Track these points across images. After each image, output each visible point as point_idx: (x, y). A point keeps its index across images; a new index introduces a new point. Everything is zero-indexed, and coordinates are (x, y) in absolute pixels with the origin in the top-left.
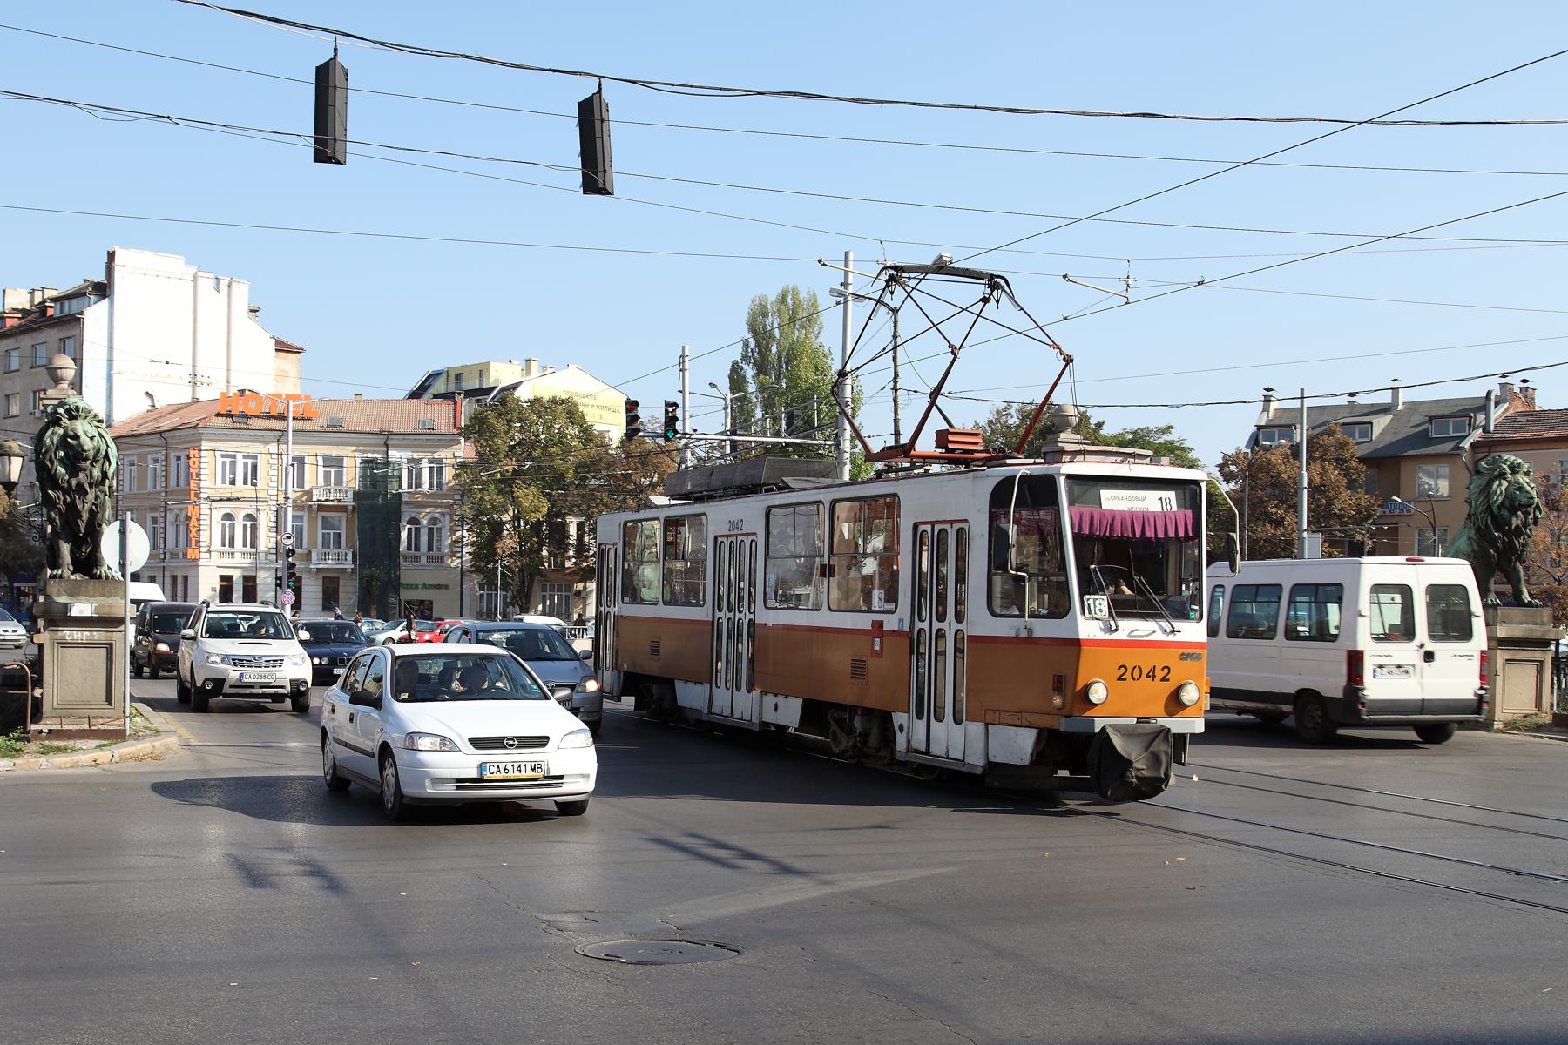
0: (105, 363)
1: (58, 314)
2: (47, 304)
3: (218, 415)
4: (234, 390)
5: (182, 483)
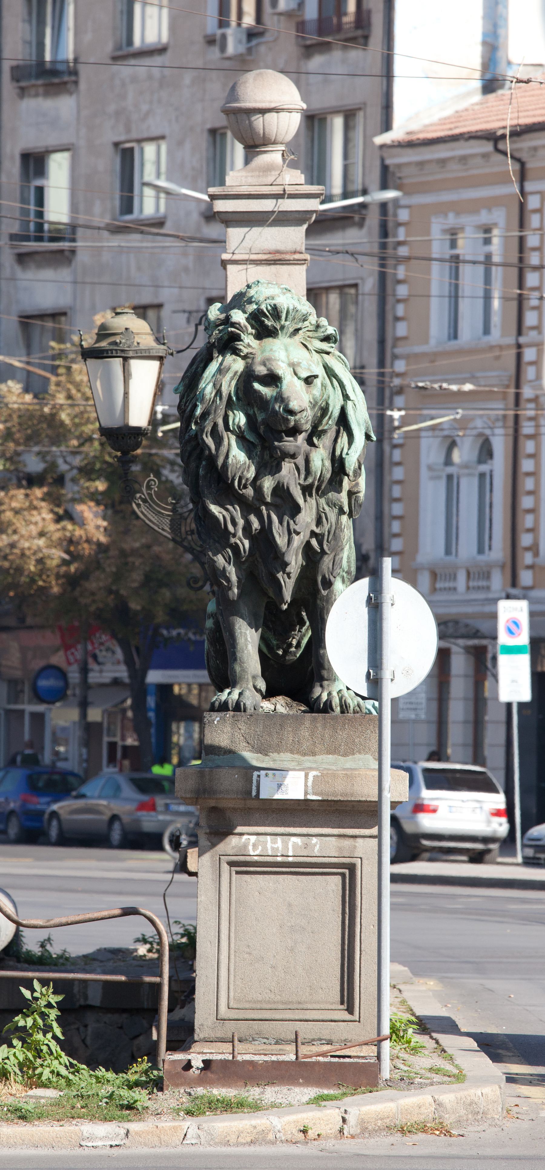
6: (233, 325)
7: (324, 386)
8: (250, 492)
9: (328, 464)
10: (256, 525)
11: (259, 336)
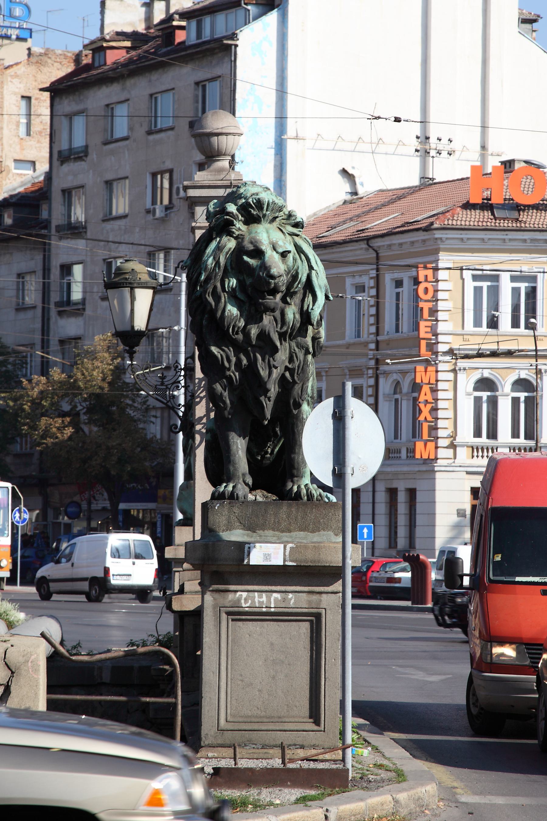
0: (272, 122)
1: (193, 40)
2: (175, 23)
3: (468, 206)
4: (493, 162)
5: (405, 326)
6: (229, 214)
7: (294, 259)
8: (240, 337)
9: (298, 316)
10: (245, 362)
11: (247, 223)
